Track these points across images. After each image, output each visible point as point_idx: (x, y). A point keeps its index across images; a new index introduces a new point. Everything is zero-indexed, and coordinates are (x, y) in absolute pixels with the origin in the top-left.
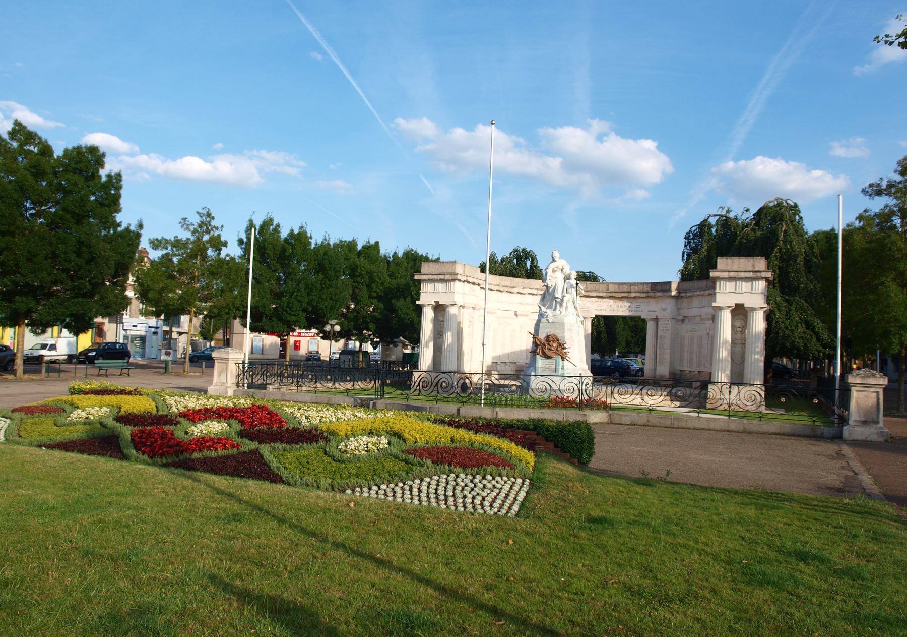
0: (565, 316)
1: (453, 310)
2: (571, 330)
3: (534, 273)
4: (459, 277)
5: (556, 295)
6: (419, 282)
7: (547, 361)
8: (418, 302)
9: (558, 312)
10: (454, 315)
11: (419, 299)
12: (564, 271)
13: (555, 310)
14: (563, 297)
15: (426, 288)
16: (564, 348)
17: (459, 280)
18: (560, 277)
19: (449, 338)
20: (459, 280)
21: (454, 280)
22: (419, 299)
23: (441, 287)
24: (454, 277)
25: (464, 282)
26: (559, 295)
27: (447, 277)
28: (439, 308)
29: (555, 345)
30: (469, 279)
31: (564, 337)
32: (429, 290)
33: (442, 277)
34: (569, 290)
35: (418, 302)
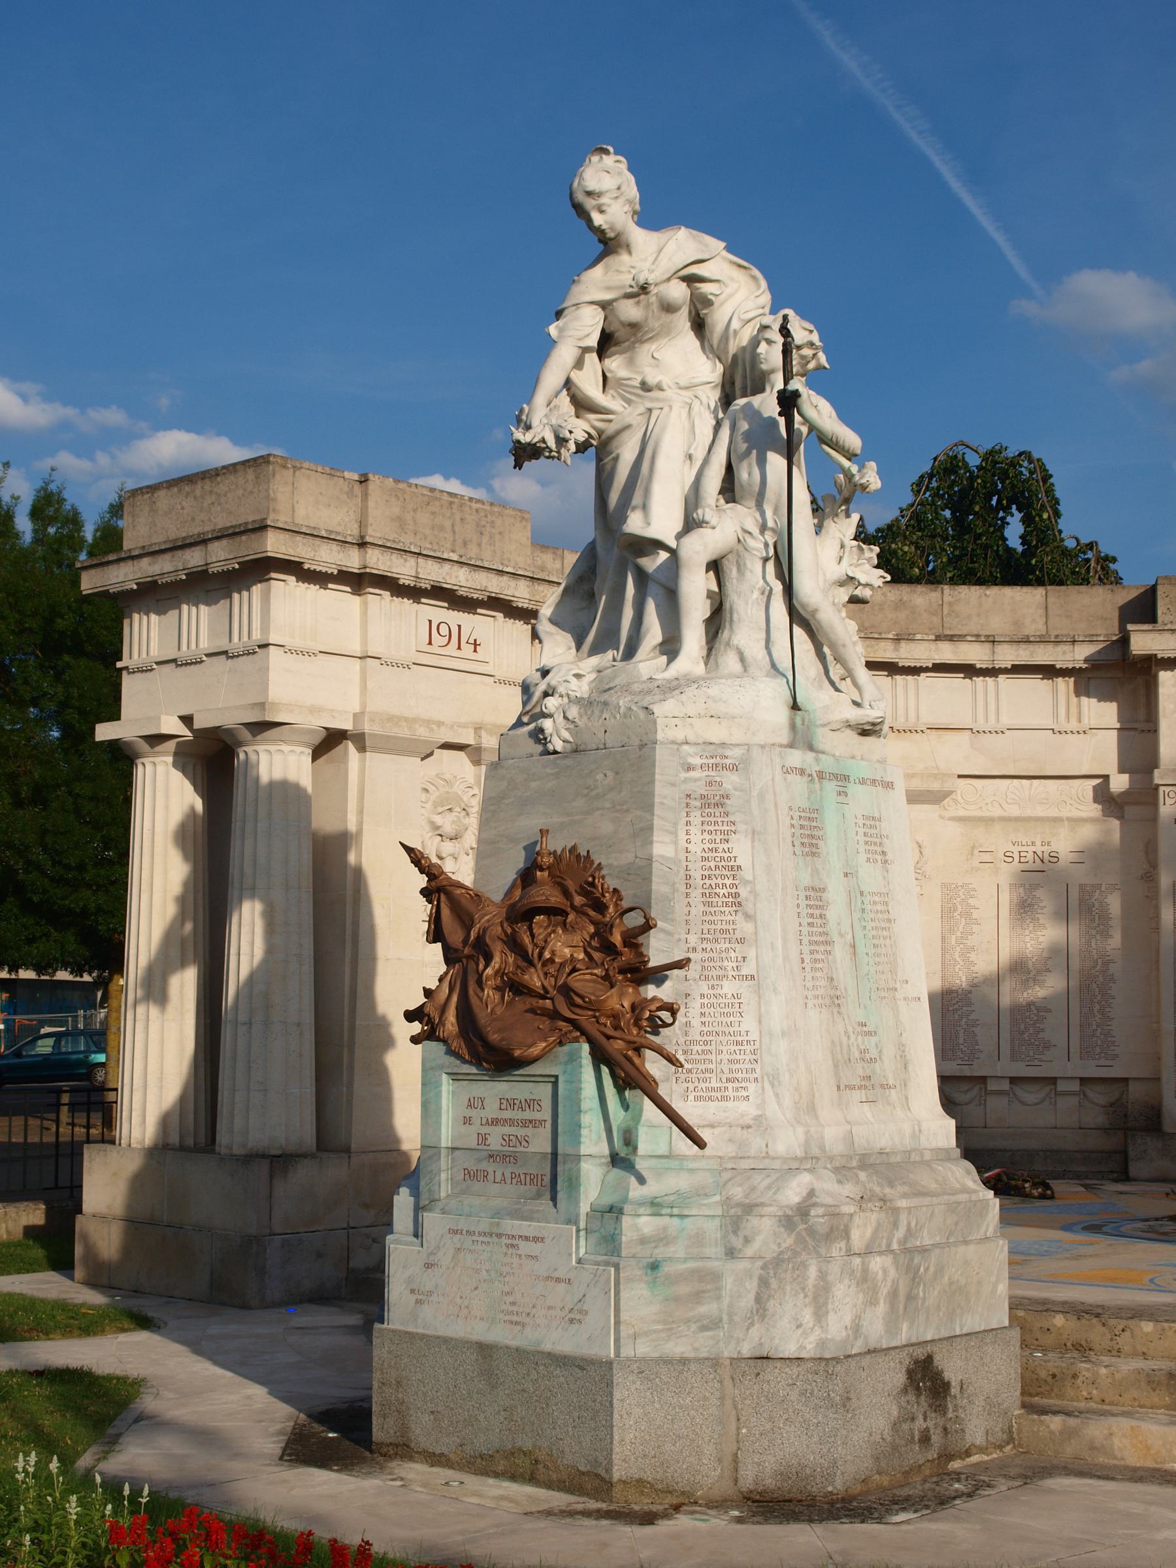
0: (673, 687)
1: (278, 763)
2: (714, 803)
3: (1045, 563)
4: (275, 545)
5: (634, 524)
6: (118, 607)
7: (495, 1090)
8: (105, 732)
9: (648, 664)
10: (287, 794)
11: (115, 716)
12: (718, 318)
13: (630, 652)
14: (691, 524)
15: (147, 636)
16: (642, 973)
17: (294, 568)
18: (681, 366)
19: (248, 938)
20: (294, 568)
21: (260, 569)
22: (115, 716)
23: (199, 624)
24: (248, 549)
25: (358, 581)
26: (659, 518)
27: (220, 556)
28: (214, 758)
29: (564, 946)
30: (378, 562)
31: (643, 871)
32: (156, 651)
33: (194, 559)
34: (747, 473)
35: (105, 732)
